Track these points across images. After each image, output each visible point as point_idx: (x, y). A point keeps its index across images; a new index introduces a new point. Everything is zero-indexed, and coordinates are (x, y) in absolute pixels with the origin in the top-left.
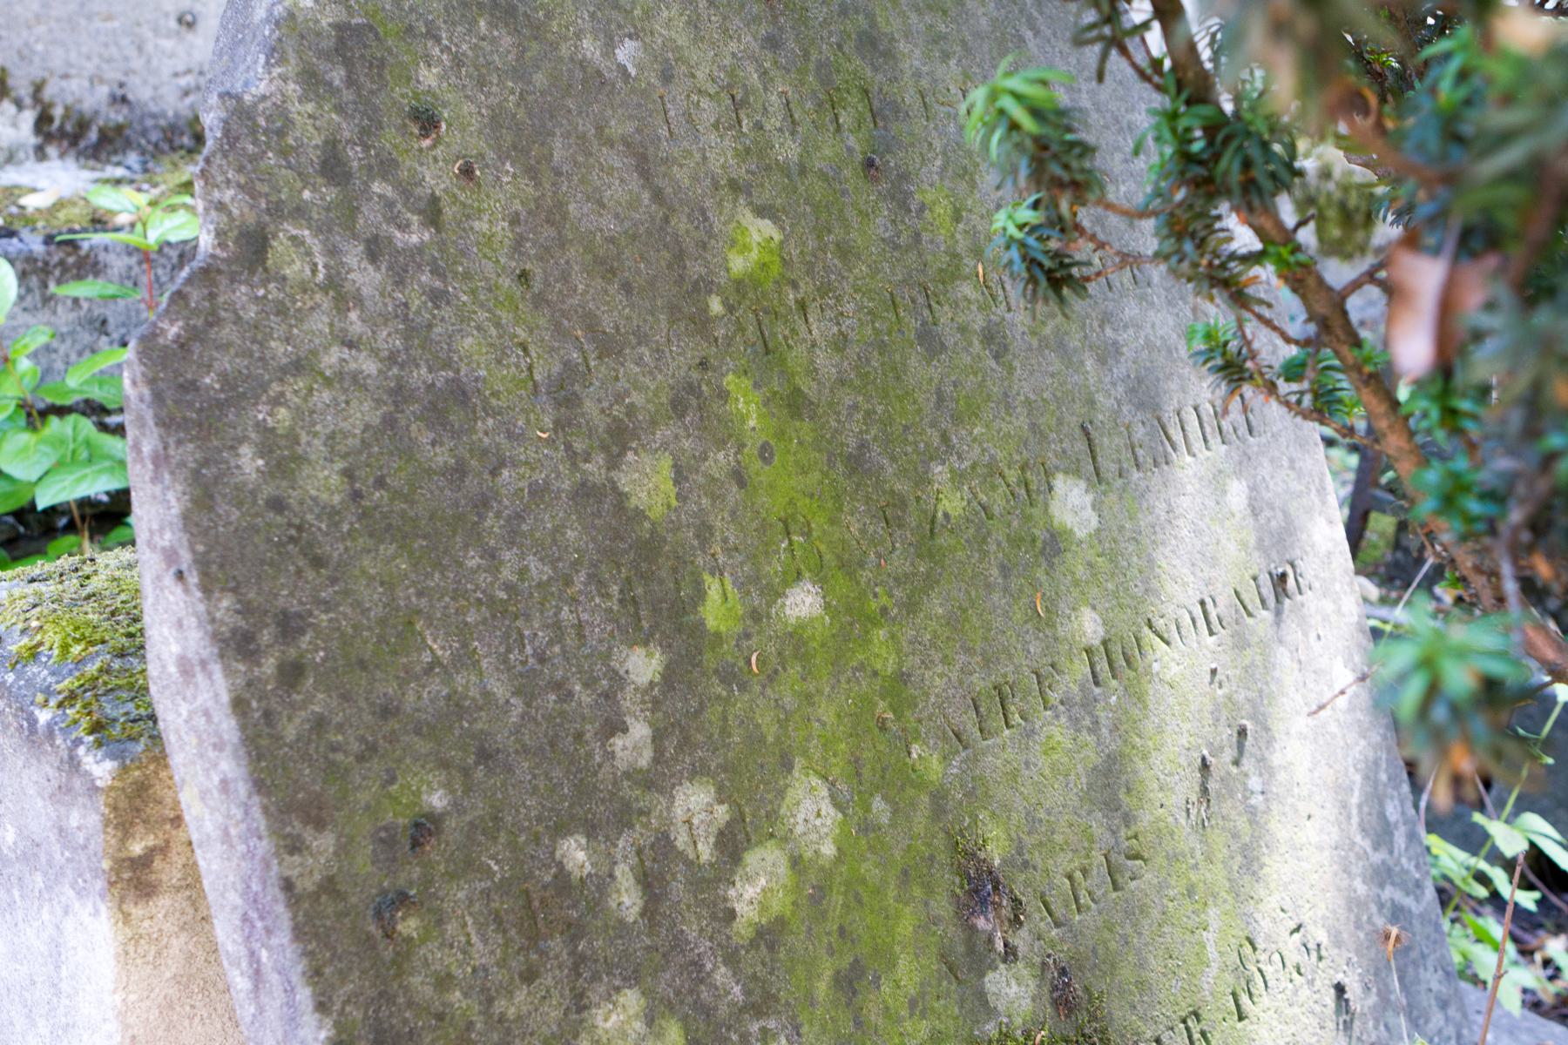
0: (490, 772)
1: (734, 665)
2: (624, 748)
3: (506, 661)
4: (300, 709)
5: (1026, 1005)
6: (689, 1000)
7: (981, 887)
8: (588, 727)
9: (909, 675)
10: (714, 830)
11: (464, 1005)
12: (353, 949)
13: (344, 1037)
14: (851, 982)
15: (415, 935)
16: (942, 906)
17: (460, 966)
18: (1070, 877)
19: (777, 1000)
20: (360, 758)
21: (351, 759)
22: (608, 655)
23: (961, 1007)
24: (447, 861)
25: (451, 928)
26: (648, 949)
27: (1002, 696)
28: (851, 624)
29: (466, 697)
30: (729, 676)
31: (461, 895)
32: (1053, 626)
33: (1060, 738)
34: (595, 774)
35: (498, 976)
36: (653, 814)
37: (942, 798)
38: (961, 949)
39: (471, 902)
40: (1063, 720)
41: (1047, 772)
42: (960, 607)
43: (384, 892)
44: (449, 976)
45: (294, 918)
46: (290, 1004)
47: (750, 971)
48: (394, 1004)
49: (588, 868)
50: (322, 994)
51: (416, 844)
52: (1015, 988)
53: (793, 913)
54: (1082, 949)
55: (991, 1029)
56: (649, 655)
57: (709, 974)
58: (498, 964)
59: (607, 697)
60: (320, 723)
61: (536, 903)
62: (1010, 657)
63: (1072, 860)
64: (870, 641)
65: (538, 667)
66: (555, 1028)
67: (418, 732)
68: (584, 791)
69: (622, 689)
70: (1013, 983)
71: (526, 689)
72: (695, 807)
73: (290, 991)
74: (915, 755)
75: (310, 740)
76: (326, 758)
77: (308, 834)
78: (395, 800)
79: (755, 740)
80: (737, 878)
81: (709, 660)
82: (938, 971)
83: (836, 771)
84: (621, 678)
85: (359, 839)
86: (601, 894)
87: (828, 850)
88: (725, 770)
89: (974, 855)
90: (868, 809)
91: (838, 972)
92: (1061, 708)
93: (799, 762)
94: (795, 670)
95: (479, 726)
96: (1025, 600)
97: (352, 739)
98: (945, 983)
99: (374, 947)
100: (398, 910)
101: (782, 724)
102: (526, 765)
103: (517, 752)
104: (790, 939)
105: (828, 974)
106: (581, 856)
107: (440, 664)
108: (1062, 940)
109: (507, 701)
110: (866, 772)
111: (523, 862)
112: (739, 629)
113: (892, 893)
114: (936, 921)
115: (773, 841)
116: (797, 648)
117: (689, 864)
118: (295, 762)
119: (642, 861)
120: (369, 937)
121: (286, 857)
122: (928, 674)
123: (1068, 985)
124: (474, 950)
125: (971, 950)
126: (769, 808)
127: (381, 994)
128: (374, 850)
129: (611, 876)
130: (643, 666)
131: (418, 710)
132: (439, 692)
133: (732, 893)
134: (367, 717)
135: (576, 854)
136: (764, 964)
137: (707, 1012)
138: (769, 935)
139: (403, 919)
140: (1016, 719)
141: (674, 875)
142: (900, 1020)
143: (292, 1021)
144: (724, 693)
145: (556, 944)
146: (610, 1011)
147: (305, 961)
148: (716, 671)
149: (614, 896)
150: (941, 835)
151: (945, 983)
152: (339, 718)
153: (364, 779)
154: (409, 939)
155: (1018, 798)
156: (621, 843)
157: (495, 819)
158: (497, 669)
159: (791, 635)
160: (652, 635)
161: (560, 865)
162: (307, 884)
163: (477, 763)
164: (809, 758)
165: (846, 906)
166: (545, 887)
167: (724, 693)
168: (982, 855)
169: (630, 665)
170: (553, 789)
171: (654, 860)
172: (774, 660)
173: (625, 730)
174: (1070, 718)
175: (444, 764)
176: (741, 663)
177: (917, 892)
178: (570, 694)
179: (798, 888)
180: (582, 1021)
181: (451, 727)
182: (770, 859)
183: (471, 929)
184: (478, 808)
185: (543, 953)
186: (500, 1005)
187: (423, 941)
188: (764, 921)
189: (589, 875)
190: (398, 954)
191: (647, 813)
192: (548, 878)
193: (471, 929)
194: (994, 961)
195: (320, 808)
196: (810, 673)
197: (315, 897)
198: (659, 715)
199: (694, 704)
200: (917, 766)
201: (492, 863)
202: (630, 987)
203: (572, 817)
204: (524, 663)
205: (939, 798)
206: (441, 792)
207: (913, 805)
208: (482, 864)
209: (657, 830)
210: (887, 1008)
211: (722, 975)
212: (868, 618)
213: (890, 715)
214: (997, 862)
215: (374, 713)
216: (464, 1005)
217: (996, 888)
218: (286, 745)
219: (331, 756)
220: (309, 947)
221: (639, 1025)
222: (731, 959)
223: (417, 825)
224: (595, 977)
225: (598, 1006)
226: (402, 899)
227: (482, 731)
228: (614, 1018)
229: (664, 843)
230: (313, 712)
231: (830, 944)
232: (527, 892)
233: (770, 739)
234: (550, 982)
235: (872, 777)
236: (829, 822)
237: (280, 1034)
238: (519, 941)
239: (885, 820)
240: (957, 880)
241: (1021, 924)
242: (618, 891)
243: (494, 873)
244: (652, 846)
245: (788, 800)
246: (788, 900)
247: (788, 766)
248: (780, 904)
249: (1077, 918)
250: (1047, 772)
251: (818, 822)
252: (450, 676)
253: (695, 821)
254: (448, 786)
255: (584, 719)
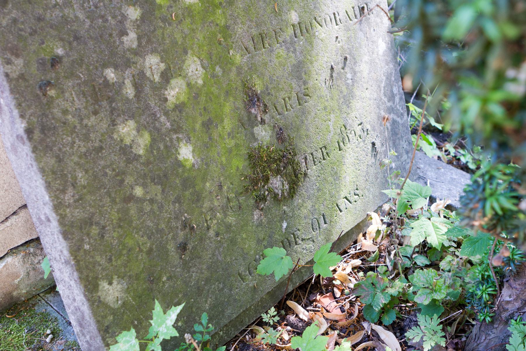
0: (79, 44)
1: (166, 16)
2: (127, 41)
3: (83, 6)
4: (7, 15)
5: (268, 138)
6: (152, 126)
7: (253, 99)
8: (114, 32)
9: (229, 27)
10: (160, 71)
11: (73, 120)
12: (32, 98)
13: (31, 127)
14: (208, 125)
15: (54, 96)
16: (240, 104)
17: (71, 107)
18: (284, 100)
19: (182, 129)
20: (31, 34)
21: (27, 34)
22: (120, 8)
23: (246, 137)
24: (64, 73)
25: (67, 95)
26: (137, 108)
27: (262, 37)
28: (209, 7)
29: (69, 17)
30: (164, 20)
31: (70, 84)
32: (281, 16)
33: (282, 54)
34: (117, 48)
35: (84, 112)
36: (138, 64)
37: (240, 69)
38: (246, 118)
39: (74, 87)
40: (283, 48)
41: (277, 64)
42: (248, 5)
43: (42, 80)
44: (67, 110)
45: (10, 86)
46: (12, 117)
47: (173, 119)
48: (48, 117)
49: (115, 79)
50: (22, 112)
51: (53, 65)
52: (264, 133)
53: (188, 101)
54: (287, 123)
55: (256, 145)
56: (136, 10)
57: (158, 118)
58: (84, 108)
59: (120, 22)
60: (15, 21)
61: (97, 89)
62: (265, 24)
63: (285, 94)
64: (215, 14)
65: (95, 9)
66: (105, 130)
67: (51, 27)
68: (113, 54)
69: (126, 20)
70: (264, 131)
71: (91, 16)
72: (153, 64)
73: (11, 112)
74: (231, 54)
75: (11, 26)
76: (18, 33)
77: (13, 58)
78: (44, 50)
79: (174, 43)
80: (168, 88)
81: (157, 13)
82: (238, 125)
83: (203, 56)
84: (125, 16)
85: (32, 62)
86: (120, 88)
87: (200, 82)
88: (163, 52)
89: (251, 89)
90: (214, 70)
91: (203, 122)
92: (283, 44)
93: (190, 52)
94: (188, 20)
95: (74, 28)
96: (271, 6)
97: (27, 28)
98: (240, 129)
99: (39, 98)
100: (47, 87)
101: (184, 38)
102: (92, 43)
103: (88, 38)
104: (187, 110)
105: (200, 122)
106: (112, 75)
107: (59, 5)
108: (281, 119)
109: (84, 20)
110: (214, 58)
111: (92, 76)
112: (168, 4)
113: (222, 98)
114: (237, 109)
115: (181, 77)
116: (189, 13)
117: (151, 82)
118: (7, 33)
119: (134, 79)
120: (38, 95)
121: (6, 65)
122: (236, 27)
123: (282, 133)
124: (75, 103)
125: (249, 119)
126: (179, 66)
127: (43, 114)
128: (38, 66)
129: (124, 83)
130: (134, 13)
131: (51, 20)
132: (59, 14)
133: (166, 92)
134: (33, 21)
135: (111, 74)
136: (178, 117)
137: (158, 130)
138: (179, 108)
139: (50, 90)
140: (267, 45)
141: (146, 85)
142: (224, 139)
143: (13, 123)
144: (163, 26)
145: (104, 103)
146: (124, 127)
147: (15, 101)
148: (160, 18)
149: (125, 90)
150: (240, 81)
151: (240, 129)
152: (22, 20)
153: (33, 41)
154: (52, 97)
155: (267, 72)
156: (127, 72)
157: (81, 60)
158: (80, 9)
159: (187, 8)
160: (137, 3)
161: (105, 78)
162: (14, 75)
163: (74, 40)
164: (193, 50)
165: (206, 101)
166: (100, 84)
167: (163, 26)
168: (254, 89)
169: (128, 12)
170: (102, 52)
171: (139, 79)
172: (181, 16)
173: (127, 35)
174: (286, 47)
175: (62, 40)
176: (169, 16)
177: (231, 99)
178: (107, 20)
179: (189, 93)
180: (114, 129)
181: (64, 27)
182: (180, 83)
183: (74, 95)
184: (75, 56)
185: (100, 106)
186: (85, 121)
187: (57, 98)
188: (178, 103)
189: (116, 82)
190: (48, 101)
191: (136, 63)
192: (101, 82)
193: (74, 95)
194: (257, 123)
195: (17, 50)
196: (194, 22)
197: (17, 80)
198: (140, 31)
199: (152, 28)
200: (232, 58)
201: (81, 75)
202: (131, 120)
203: (109, 62)
204: (90, 8)
205: (239, 69)
206: (61, 49)
207: (230, 70)
208: (77, 74)
209: (140, 69)
210: (220, 135)
211: (163, 119)
212: (215, 5)
213: (222, 40)
214: (259, 92)
215: (35, 19)
216: (73, 120)
217: (258, 100)
218: (3, 27)
219: (20, 32)
220: (16, 96)
221: (134, 132)
222: (166, 114)
223: (53, 59)
224: (119, 115)
225: (120, 125)
226: (49, 84)
227: (75, 30)
228: (125, 129)
229: (142, 74)
230: (12, 17)
231: (201, 112)
232: (94, 86)
233: (180, 43)
234: (103, 115)
235: (217, 59)
236: (200, 73)
237: (10, 129)
238: (91, 101)
239: (220, 74)
240: (245, 96)
241: (267, 112)
242: (126, 88)
243: (82, 78)
244: (138, 75)
245: (186, 64)
246: (186, 97)
247: (186, 53)
248: (183, 98)
249: (286, 113)
250: (277, 64)
251: (197, 72)
252: (63, 9)
253: (153, 68)
254: (64, 47)
255: (112, 29)
